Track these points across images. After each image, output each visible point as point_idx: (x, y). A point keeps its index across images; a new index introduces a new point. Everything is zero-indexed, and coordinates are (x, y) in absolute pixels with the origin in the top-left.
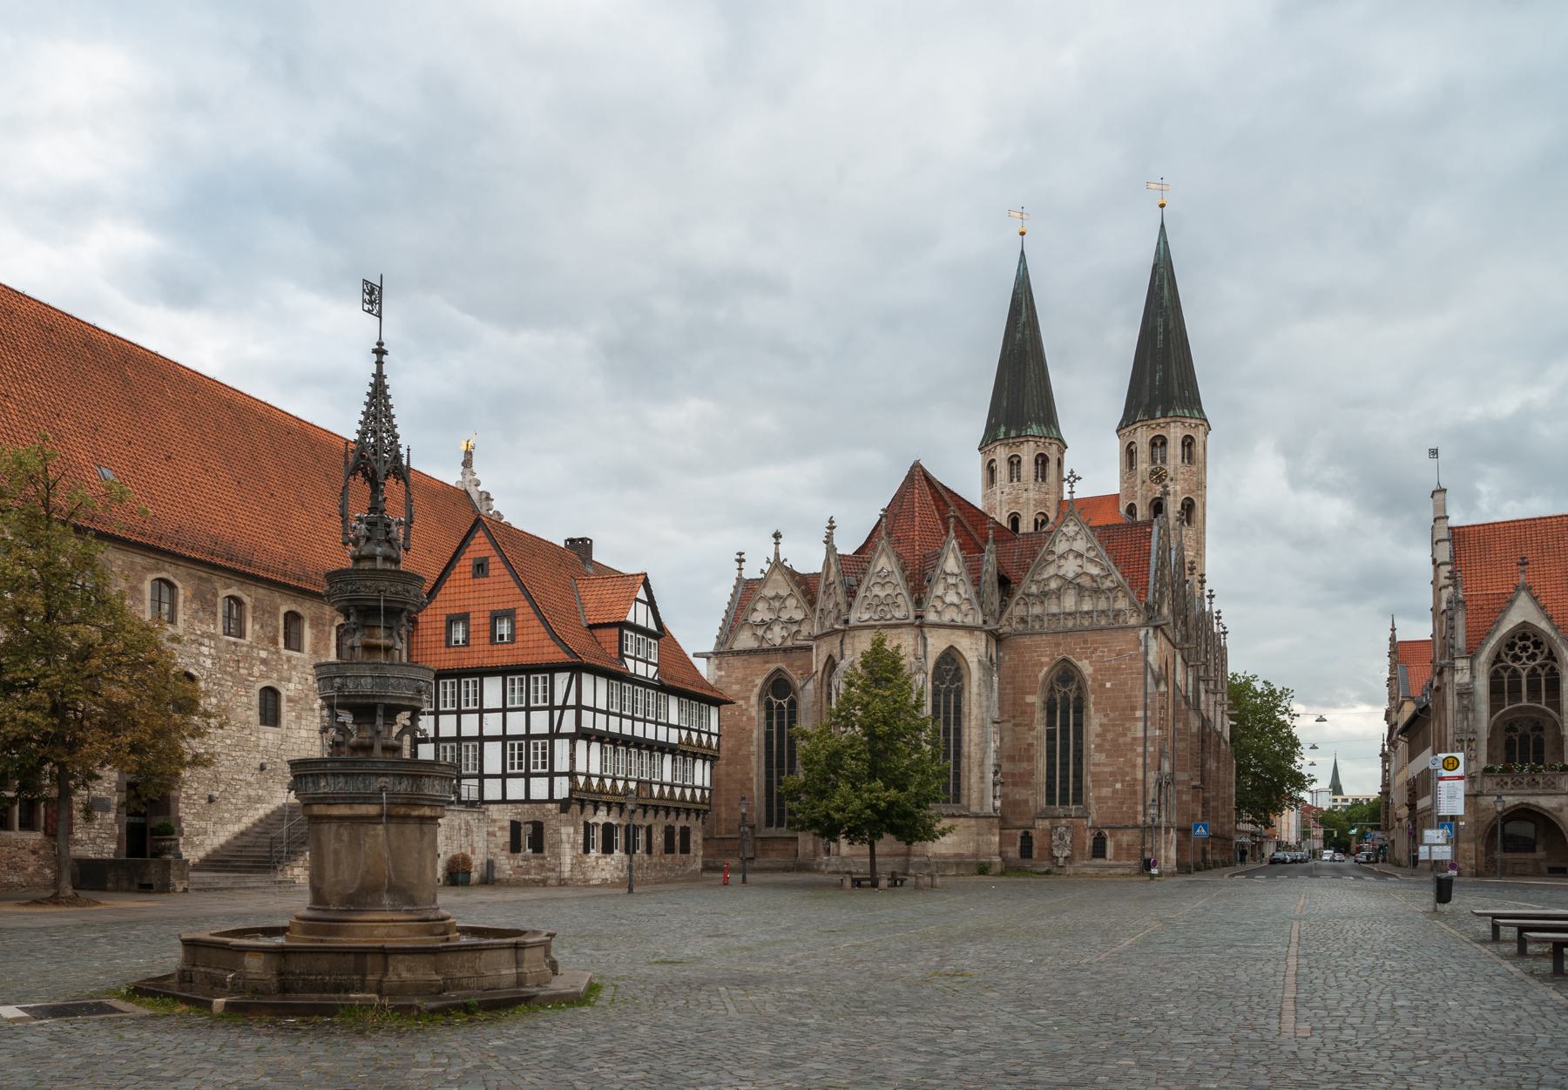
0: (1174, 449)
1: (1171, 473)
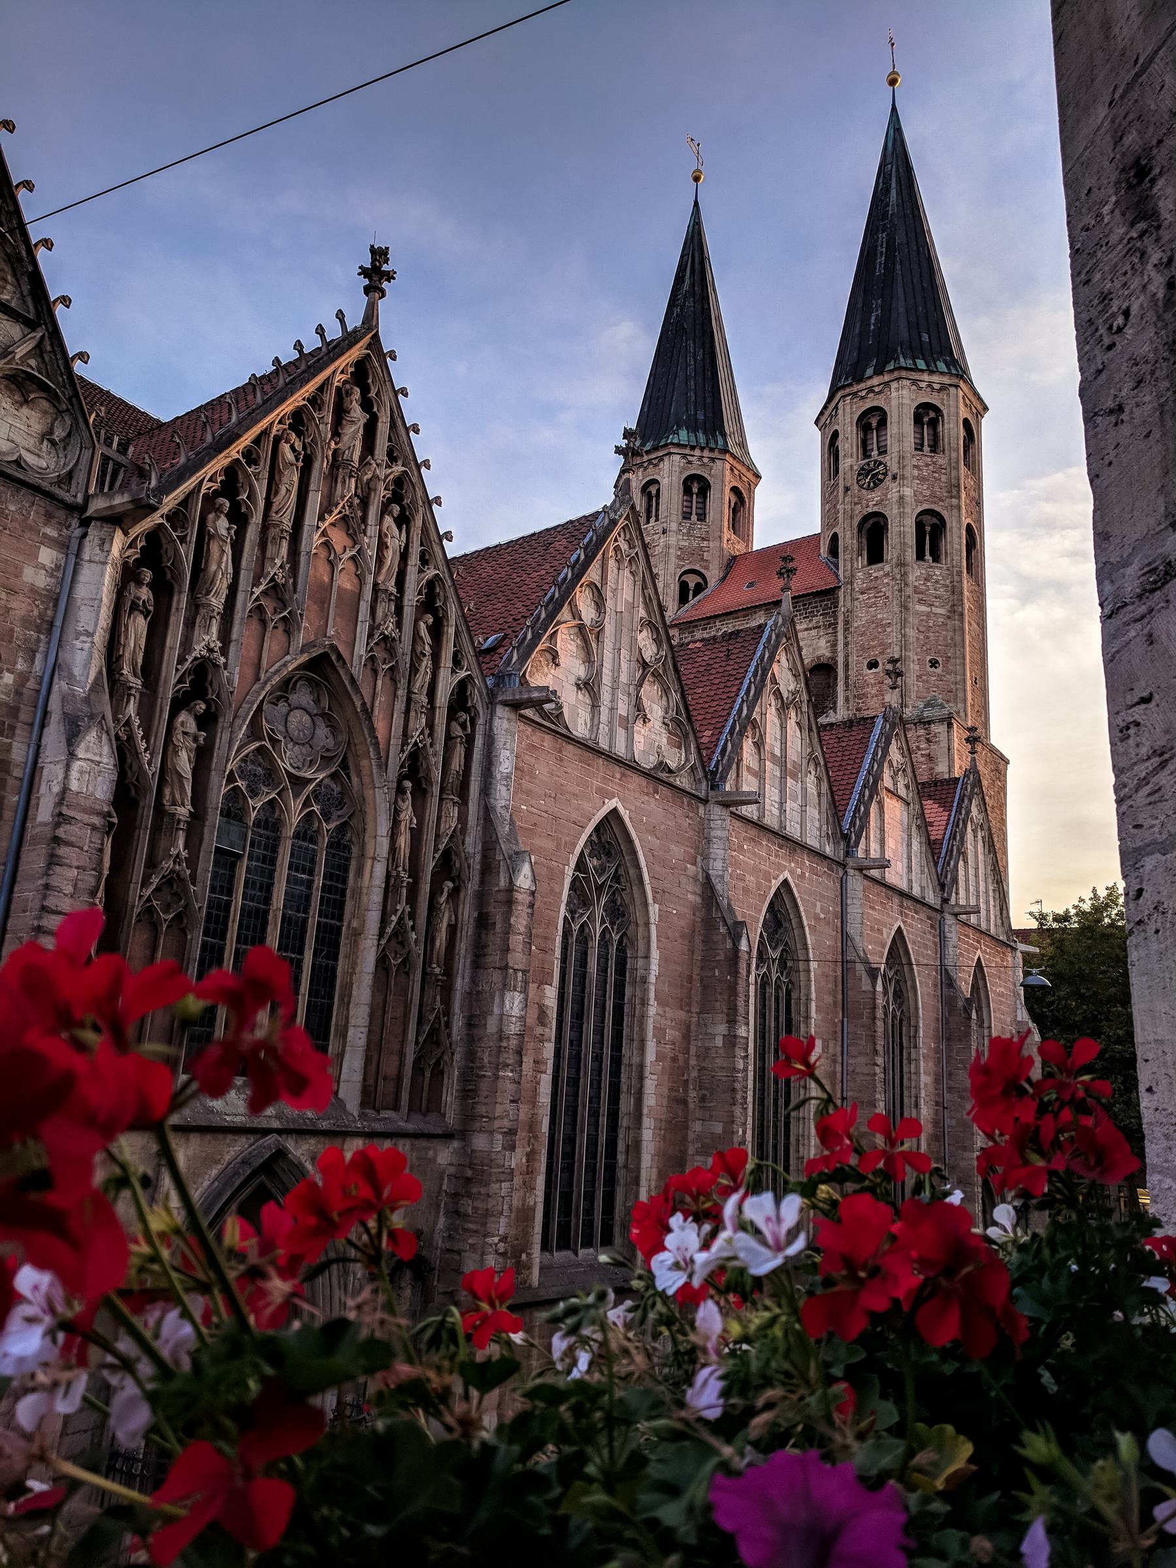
0: (901, 431)
1: (894, 468)
